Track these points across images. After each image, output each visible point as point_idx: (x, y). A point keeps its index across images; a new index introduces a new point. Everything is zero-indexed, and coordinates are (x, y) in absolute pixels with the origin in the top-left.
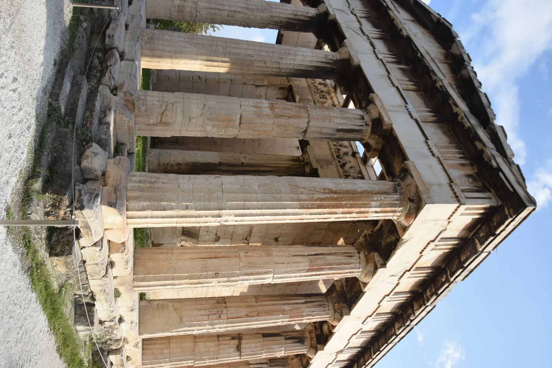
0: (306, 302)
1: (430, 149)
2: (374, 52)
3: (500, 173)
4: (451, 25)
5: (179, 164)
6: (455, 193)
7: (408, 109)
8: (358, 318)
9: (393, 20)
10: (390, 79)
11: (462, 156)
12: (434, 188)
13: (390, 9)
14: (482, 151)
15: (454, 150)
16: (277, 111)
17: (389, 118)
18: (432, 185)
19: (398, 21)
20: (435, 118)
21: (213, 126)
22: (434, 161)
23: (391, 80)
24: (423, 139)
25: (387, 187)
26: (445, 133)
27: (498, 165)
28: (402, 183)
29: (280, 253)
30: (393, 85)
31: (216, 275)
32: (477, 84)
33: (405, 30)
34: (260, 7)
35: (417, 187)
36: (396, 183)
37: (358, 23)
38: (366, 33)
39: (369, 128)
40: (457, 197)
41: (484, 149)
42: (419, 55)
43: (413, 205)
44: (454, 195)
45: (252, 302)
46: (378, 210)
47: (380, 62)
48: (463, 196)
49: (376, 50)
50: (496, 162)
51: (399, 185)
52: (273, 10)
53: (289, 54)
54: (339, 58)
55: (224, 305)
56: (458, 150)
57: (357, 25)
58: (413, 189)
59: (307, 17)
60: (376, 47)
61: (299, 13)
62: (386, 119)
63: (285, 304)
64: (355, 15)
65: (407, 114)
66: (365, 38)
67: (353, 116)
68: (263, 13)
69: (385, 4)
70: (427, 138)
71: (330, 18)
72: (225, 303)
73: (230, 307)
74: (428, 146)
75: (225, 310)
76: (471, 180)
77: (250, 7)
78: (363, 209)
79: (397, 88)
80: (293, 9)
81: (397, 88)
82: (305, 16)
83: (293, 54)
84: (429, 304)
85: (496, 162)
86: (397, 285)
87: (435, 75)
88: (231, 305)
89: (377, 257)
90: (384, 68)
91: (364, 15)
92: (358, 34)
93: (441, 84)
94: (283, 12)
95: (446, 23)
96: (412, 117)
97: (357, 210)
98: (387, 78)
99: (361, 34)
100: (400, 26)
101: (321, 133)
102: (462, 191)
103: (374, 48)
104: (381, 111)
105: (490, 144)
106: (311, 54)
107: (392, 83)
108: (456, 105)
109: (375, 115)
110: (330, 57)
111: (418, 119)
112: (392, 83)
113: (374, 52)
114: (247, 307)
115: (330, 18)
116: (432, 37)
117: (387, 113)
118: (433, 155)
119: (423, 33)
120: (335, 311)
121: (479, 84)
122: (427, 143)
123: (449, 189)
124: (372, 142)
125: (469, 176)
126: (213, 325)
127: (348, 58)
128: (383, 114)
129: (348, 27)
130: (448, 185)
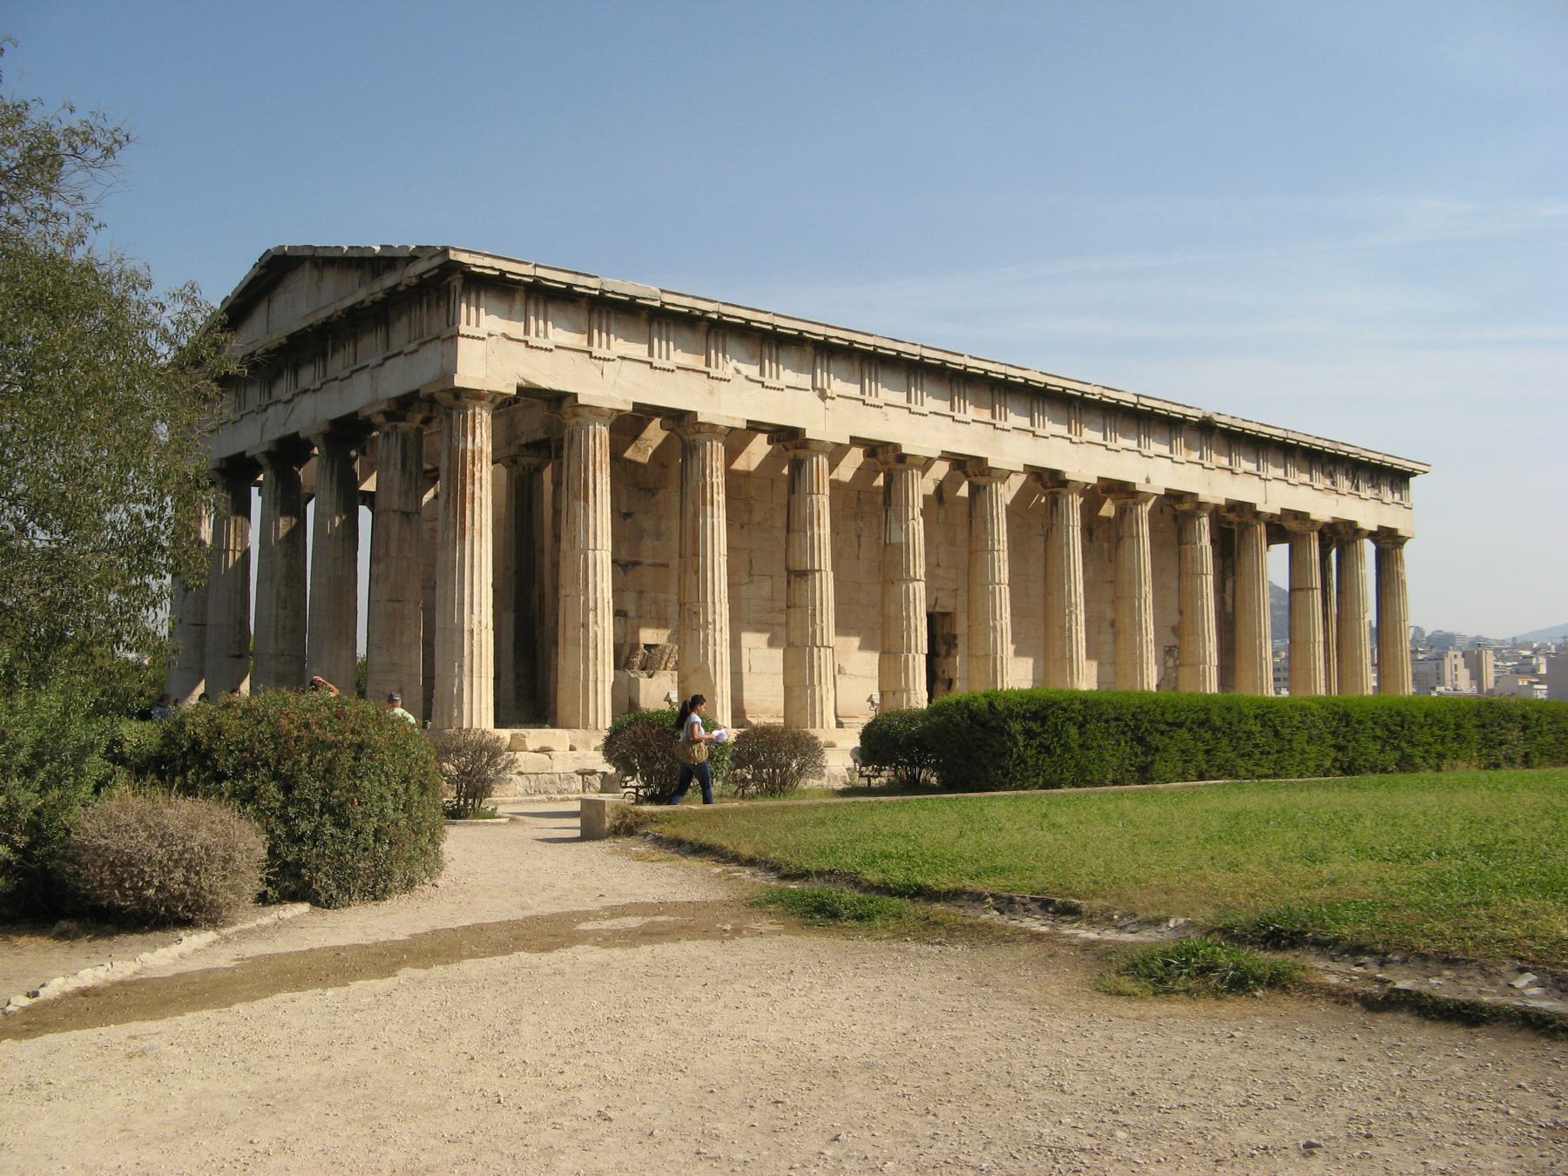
5: (517, 677)
8: (711, 393)
21: (402, 633)
31: (585, 626)
38: (288, 396)
39: (402, 425)
43: (463, 395)
46: (470, 438)
57: (280, 407)
58: (445, 395)
62: (383, 407)
71: (274, 449)
78: (469, 458)
84: (658, 304)
86: (623, 358)
89: (567, 403)
97: (469, 466)
101: (406, 493)
115: (274, 449)
120: (698, 432)
124: (419, 417)
126: (707, 622)
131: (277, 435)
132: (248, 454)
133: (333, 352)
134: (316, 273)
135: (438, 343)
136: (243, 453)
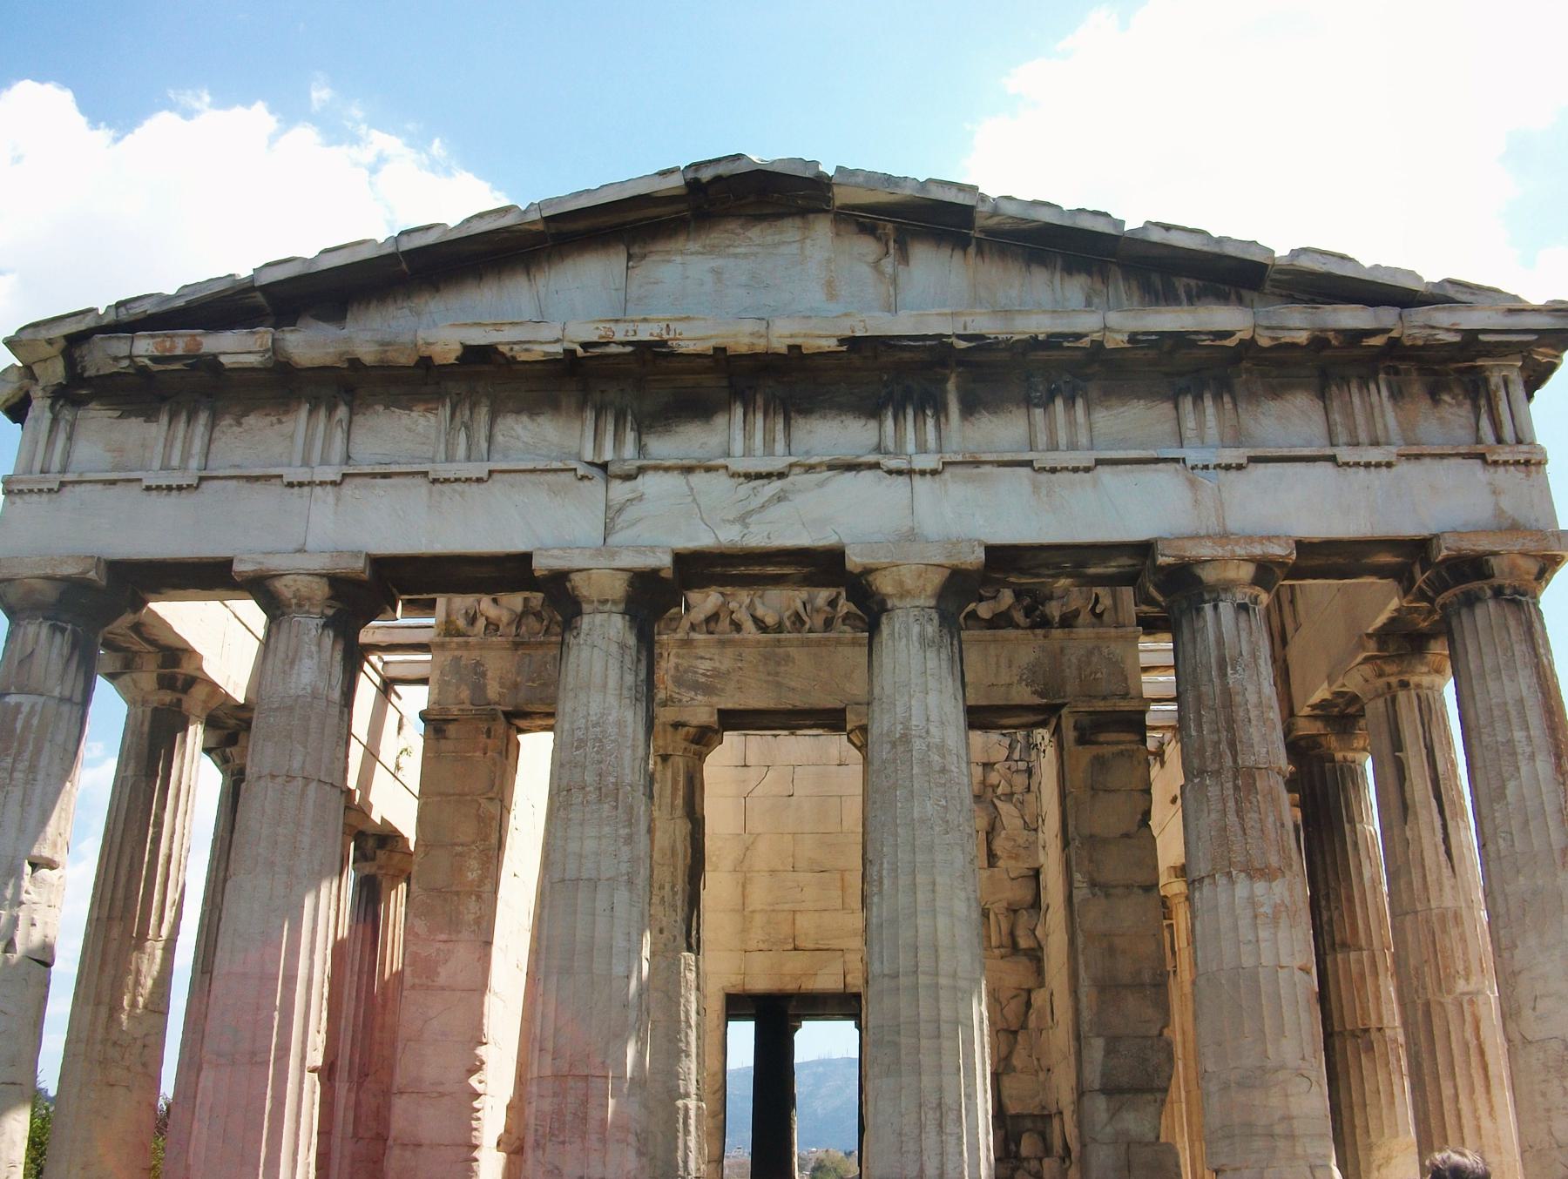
0: (1351, 821)
1: (1368, 465)
2: (900, 472)
3: (1482, 337)
4: (739, 157)
6: (1517, 463)
7: (1206, 467)
9: (720, 351)
10: (1053, 470)
11: (1372, 387)
12: (1506, 504)
13: (663, 343)
14: (1394, 343)
15: (1356, 400)
16: (1274, 860)
17: (1269, 538)
18: (1499, 512)
19: (747, 340)
20: (1227, 398)
22: (1404, 468)
23: (1066, 469)
24: (1328, 467)
25: (1512, 623)
26: (1276, 392)
27: (1457, 331)
28: (1496, 582)
29: (1447, 889)
30: (1087, 470)
32: (1100, 226)
33: (805, 336)
34: (623, 832)
35: (1524, 554)
36: (1489, 593)
37: (698, 479)
38: (778, 464)
40: (1527, 463)
41: (1394, 334)
42: (963, 345)
44: (1522, 468)
45: (1360, 961)
47: (949, 470)
48: (1523, 448)
49: (893, 463)
50: (1448, 330)
51: (1498, 592)
52: (628, 779)
53: (943, 770)
54: (933, 603)
55: (1374, 1035)
56: (1354, 390)
59: (638, 651)
60: (872, 458)
61: (629, 679)
62: (1277, 550)
63: (1360, 874)
64: (641, 470)
65: (1222, 473)
66: (797, 479)
67: (1244, 635)
68: (638, 820)
69: (613, 349)
70: (1332, 459)
72: (1367, 1030)
73: (1380, 1018)
74: (1357, 464)
75: (1388, 1032)
76: (1446, 398)
77: (624, 868)
79: (1099, 462)
80: (612, 700)
81: (1099, 462)
82: (639, 660)
83: (943, 757)
85: (1448, 330)
87: (1078, 336)
88: (1373, 1017)
90: (987, 469)
91: (630, 436)
92: (780, 498)
93: (1126, 338)
94: (629, 743)
95: (722, 170)
96: (1240, 467)
98: (1044, 477)
99: (777, 485)
100: (780, 345)
102: (1500, 440)
103: (876, 466)
104: (1240, 551)
105: (1386, 317)
106: (932, 699)
107: (1076, 470)
108: (1230, 334)
109: (1247, 572)
110: (931, 629)
111: (1252, 453)
112: (1076, 470)
113: (900, 472)
114: (1376, 975)
116: (733, 225)
117: (1250, 539)
118: (1389, 465)
119: (712, 250)
121: (1102, 220)
122: (1347, 464)
123: (1501, 470)
125: (1434, 395)
127: (947, 572)
128: (1257, 550)
129: (743, 519)
130: (1492, 470)
131: (703, 540)
132: (541, 564)
133: (970, 408)
134: (867, 247)
135: (1476, 464)
136: (526, 558)
